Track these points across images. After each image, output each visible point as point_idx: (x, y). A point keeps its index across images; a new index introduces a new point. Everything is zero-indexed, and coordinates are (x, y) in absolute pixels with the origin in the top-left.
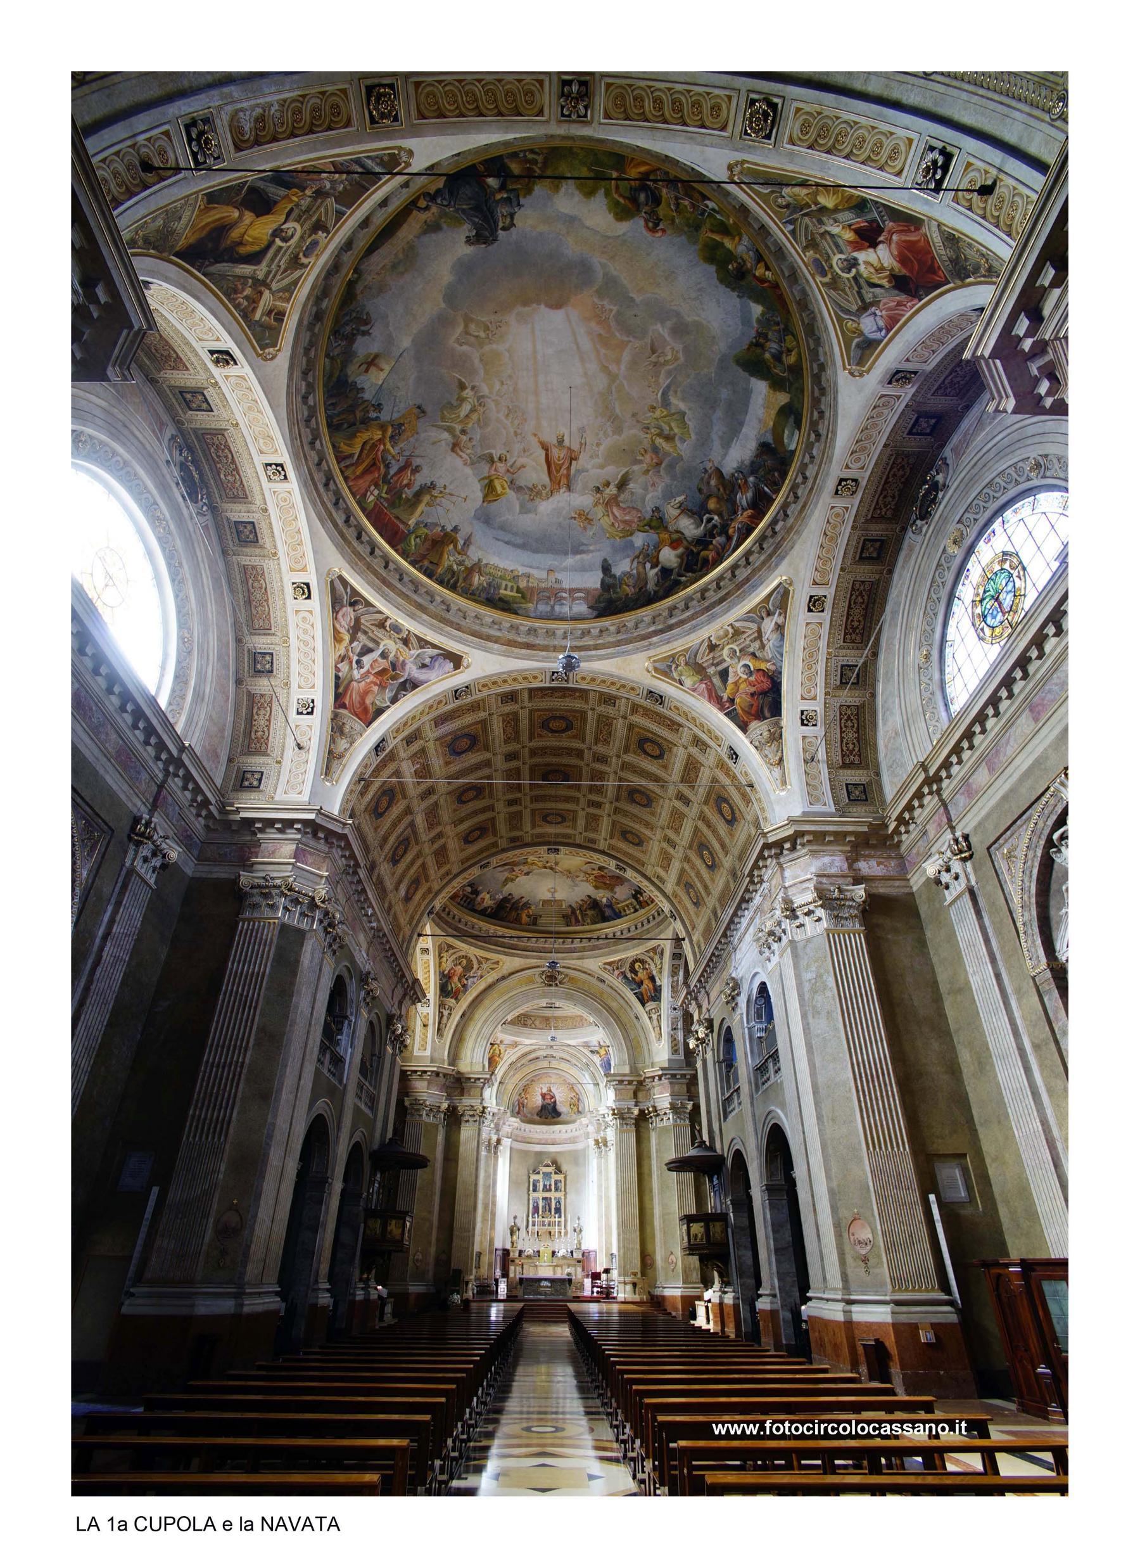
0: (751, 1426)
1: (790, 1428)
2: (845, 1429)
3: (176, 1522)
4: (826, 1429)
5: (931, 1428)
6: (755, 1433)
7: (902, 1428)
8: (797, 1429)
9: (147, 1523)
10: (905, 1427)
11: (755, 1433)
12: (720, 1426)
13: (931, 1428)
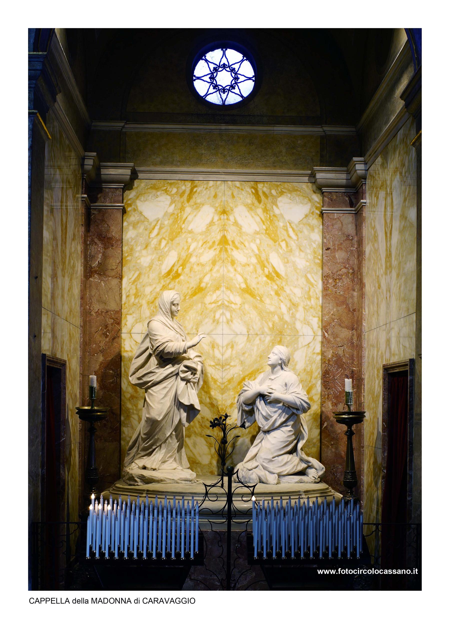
0: (333, 570)
1: (348, 571)
2: (370, 572)
4: (362, 571)
5: (404, 571)
6: (334, 573)
7: (392, 571)
8: (351, 572)
10: (393, 571)
11: (334, 573)
12: (320, 570)
13: (404, 571)
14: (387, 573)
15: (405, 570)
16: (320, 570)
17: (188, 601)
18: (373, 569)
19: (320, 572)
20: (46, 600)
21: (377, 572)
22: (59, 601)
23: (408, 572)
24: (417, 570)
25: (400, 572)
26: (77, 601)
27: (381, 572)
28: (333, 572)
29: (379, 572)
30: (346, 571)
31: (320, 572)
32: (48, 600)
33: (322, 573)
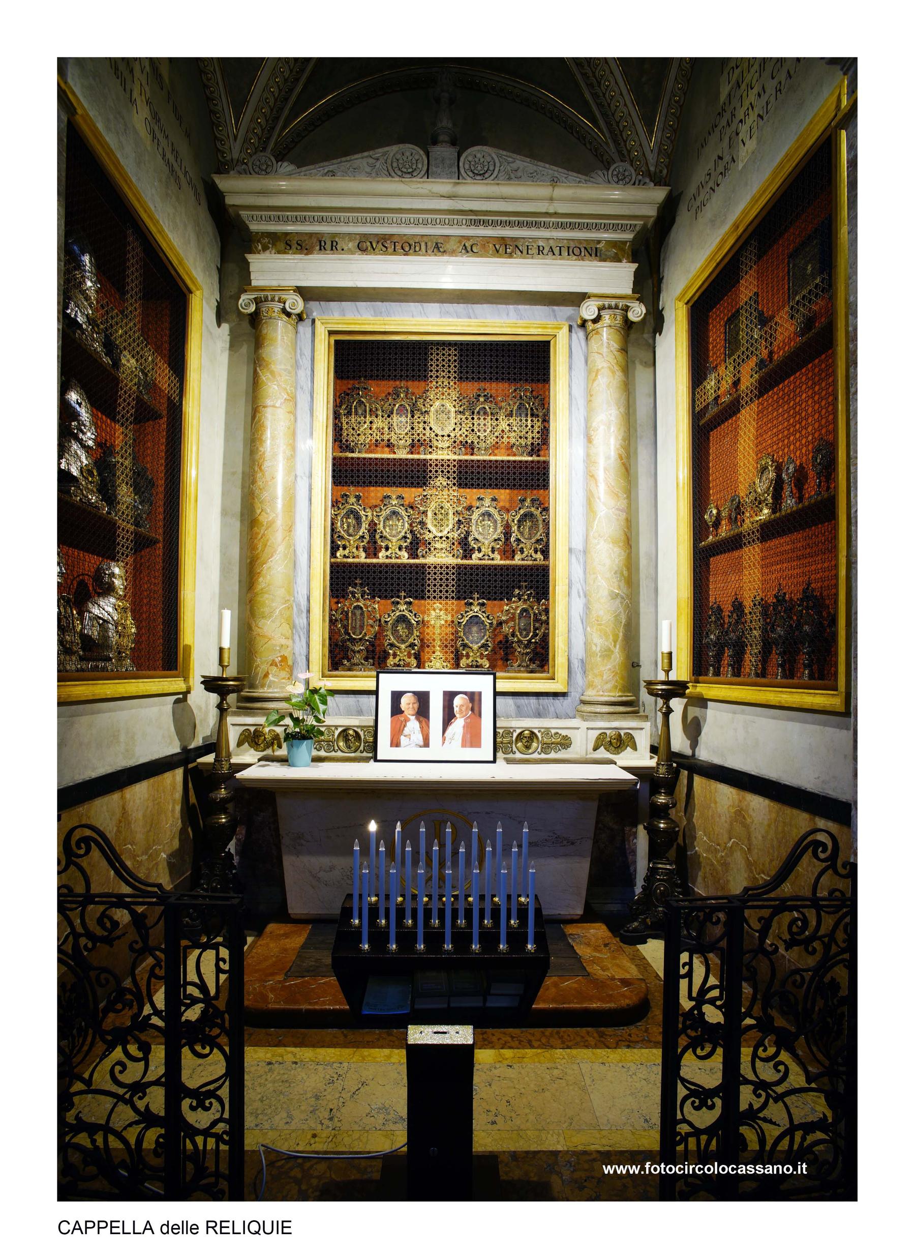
0: (634, 1167)
1: (665, 1169)
2: (709, 1169)
4: (694, 1169)
5: (778, 1168)
6: (637, 1172)
7: (755, 1168)
8: (671, 1169)
11: (637, 1172)
12: (609, 1167)
13: (778, 1168)
15: (780, 1167)
16: (609, 1167)
17: (283, 1227)
20: (99, 1226)
21: (723, 1169)
22: (129, 1229)
23: (788, 1169)
24: (804, 1166)
25: (770, 1170)
26: (171, 1229)
27: (733, 1169)
29: (729, 1169)
32: (102, 1225)
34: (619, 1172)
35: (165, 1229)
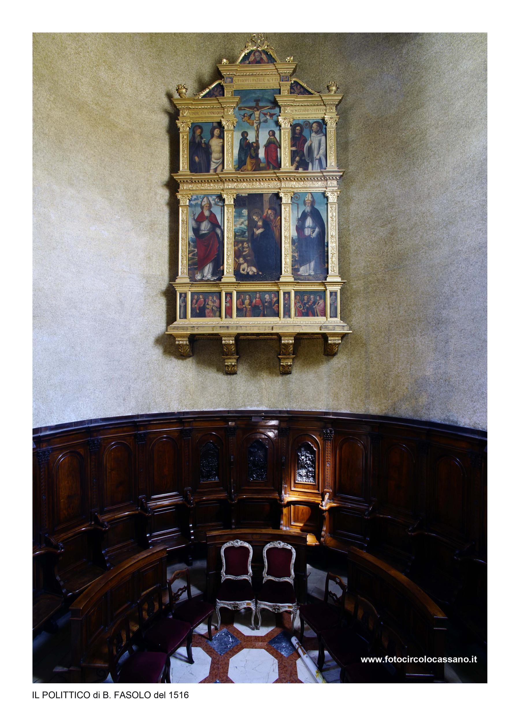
0: (379, 658)
1: (396, 660)
2: (421, 660)
3: (48, 694)
5: (460, 659)
6: (380, 662)
7: (447, 659)
8: (399, 660)
9: (83, 695)
11: (380, 662)
12: (364, 658)
13: (460, 659)
14: (441, 661)
16: (364, 658)
18: (425, 657)
19: (364, 660)
21: (429, 660)
23: (466, 660)
24: (475, 658)
27: (435, 660)
28: (379, 660)
29: (432, 660)
30: (394, 659)
31: (364, 660)
33: (366, 661)
34: (370, 662)
35: (95, 696)
